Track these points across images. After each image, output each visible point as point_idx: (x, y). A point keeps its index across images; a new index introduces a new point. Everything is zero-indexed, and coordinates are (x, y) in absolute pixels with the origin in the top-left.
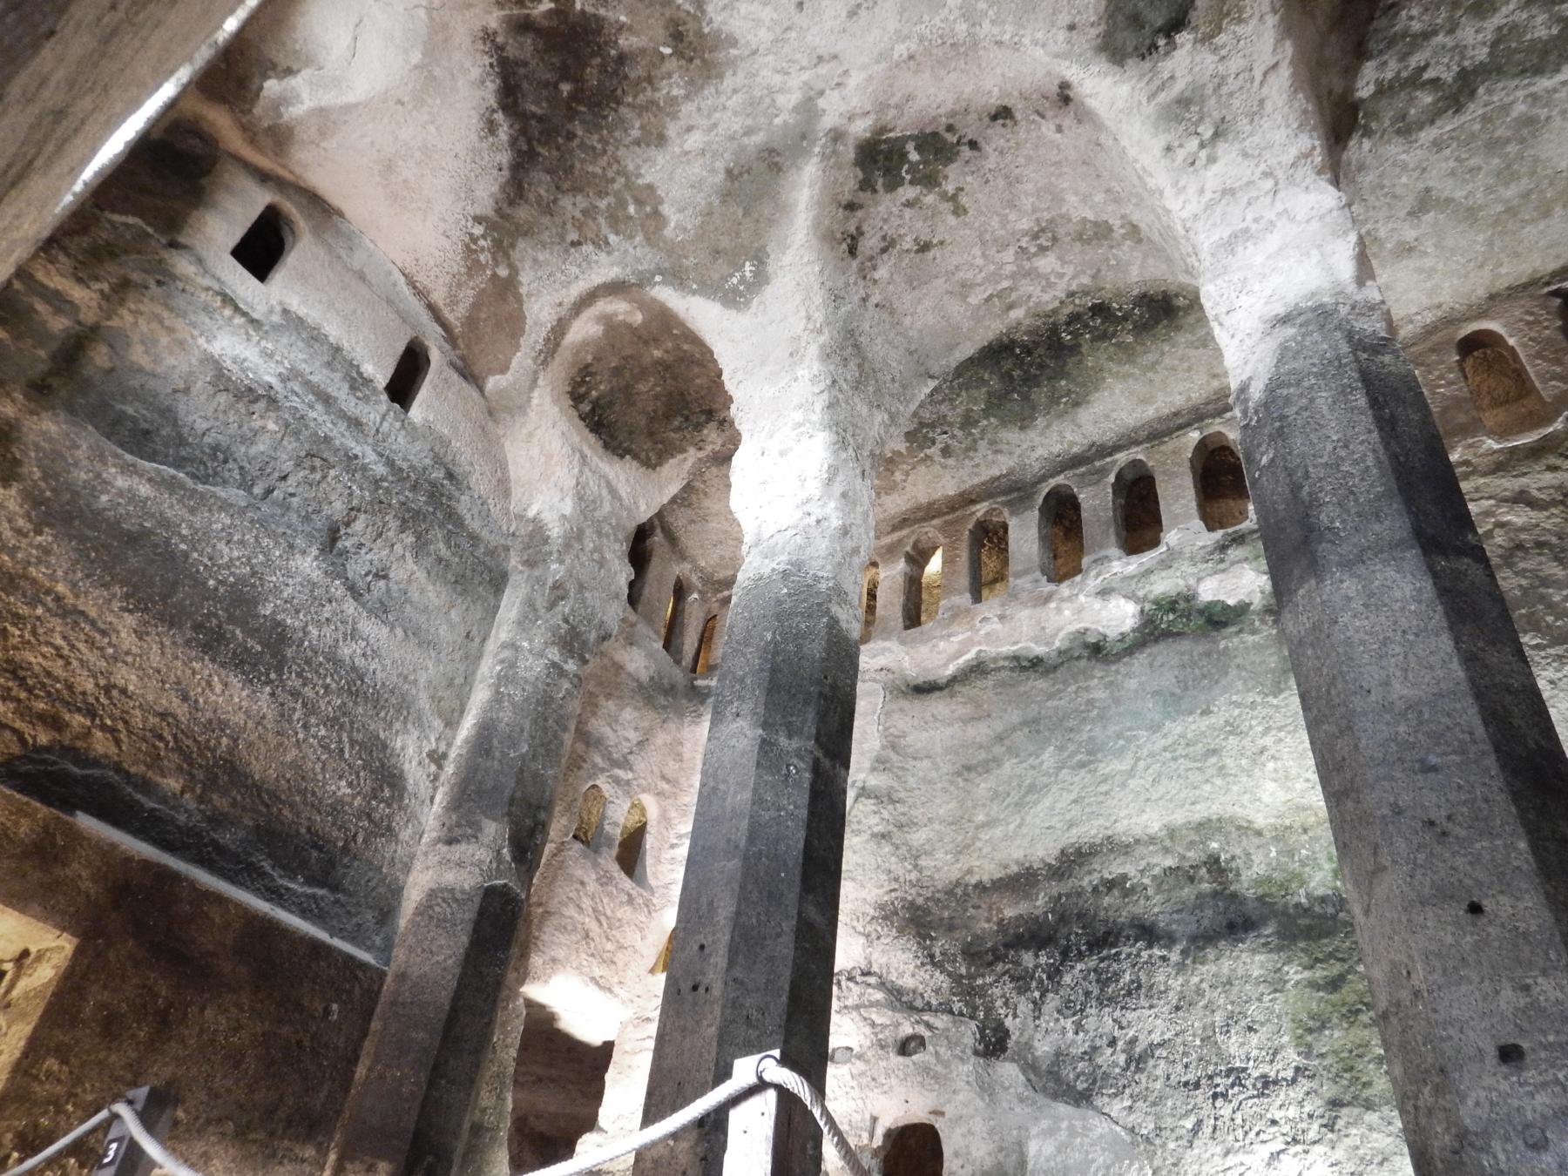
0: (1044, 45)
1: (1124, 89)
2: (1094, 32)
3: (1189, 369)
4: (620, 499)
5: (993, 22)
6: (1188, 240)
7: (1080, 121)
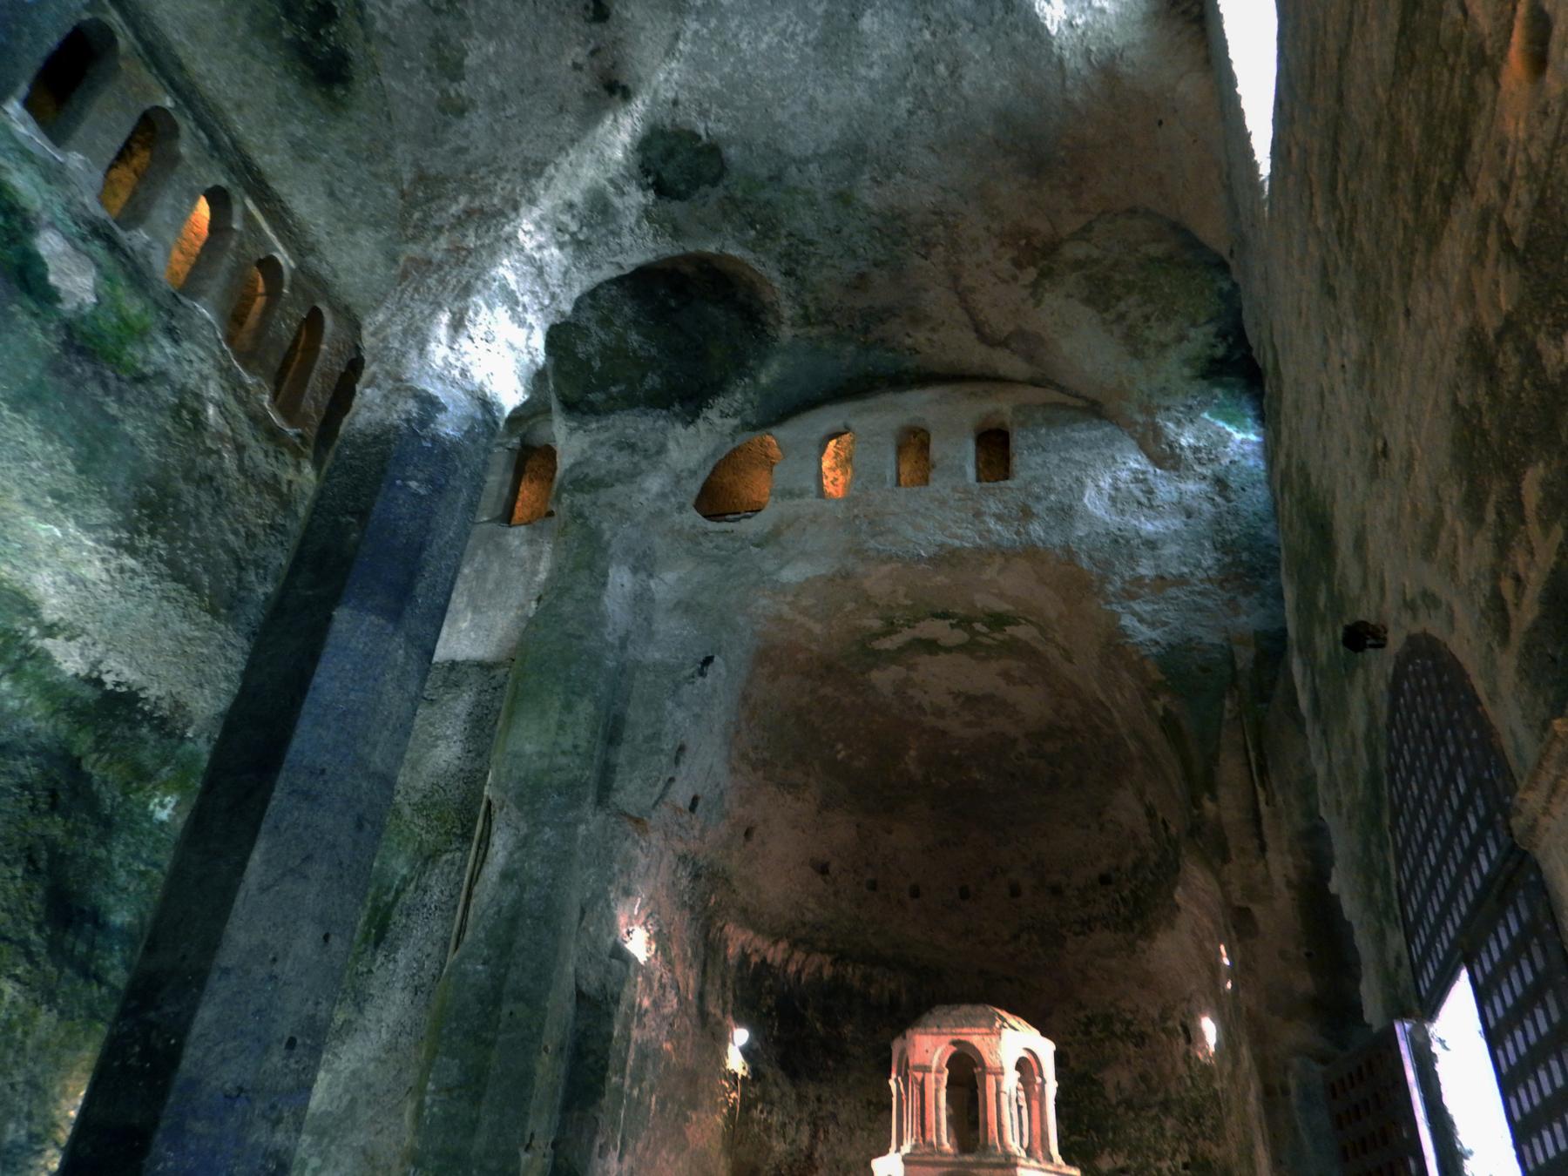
0: (666, 80)
1: (619, 155)
2: (667, 122)
3: (245, 83)
5: (696, 32)
6: (497, 239)
7: (587, 96)
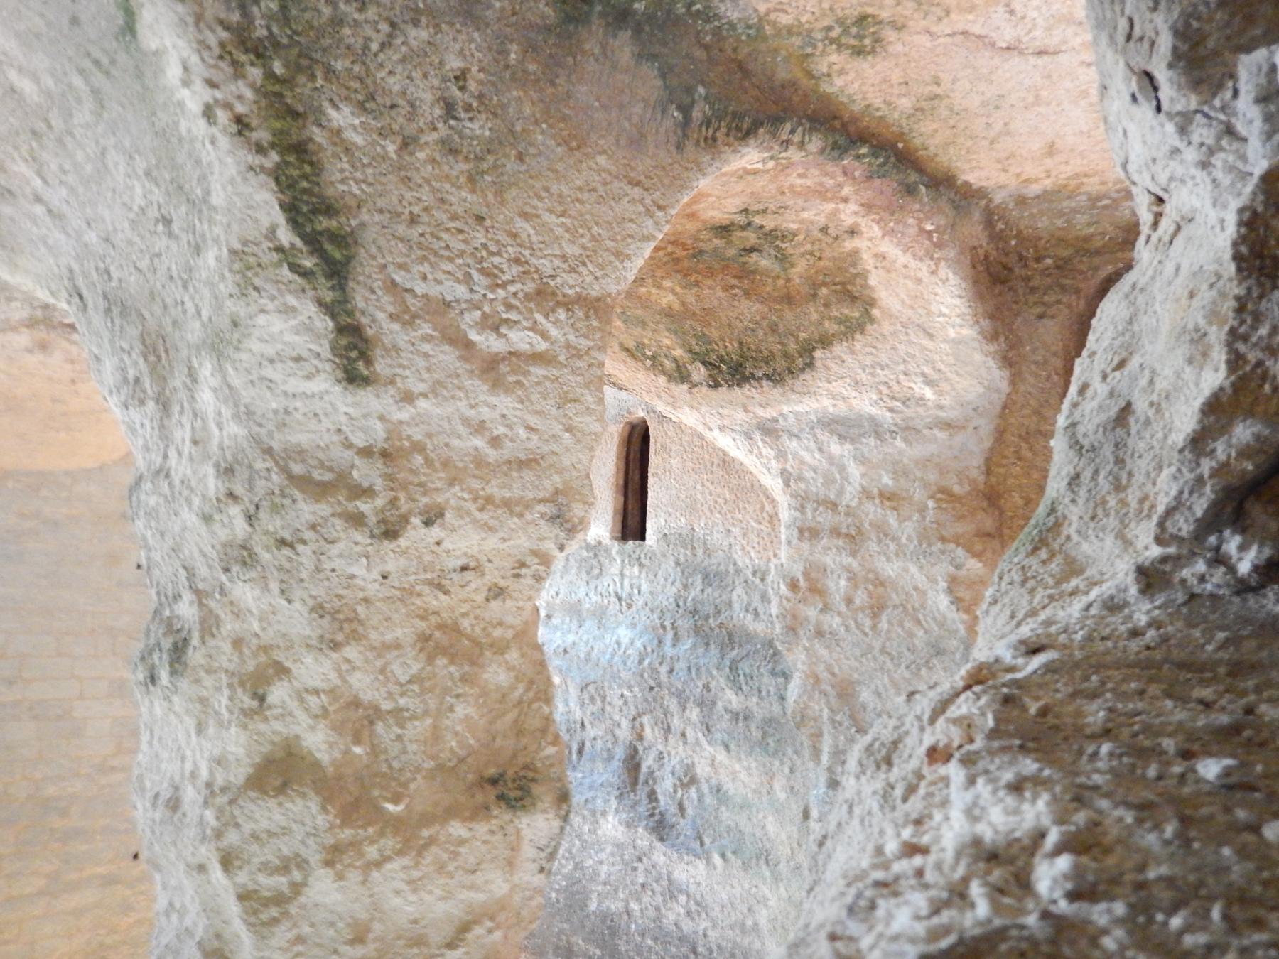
4: (877, 430)
